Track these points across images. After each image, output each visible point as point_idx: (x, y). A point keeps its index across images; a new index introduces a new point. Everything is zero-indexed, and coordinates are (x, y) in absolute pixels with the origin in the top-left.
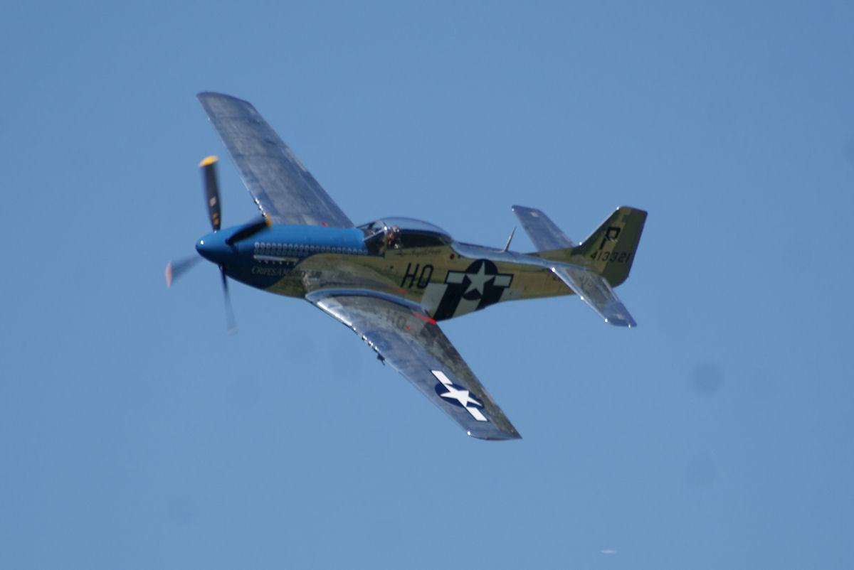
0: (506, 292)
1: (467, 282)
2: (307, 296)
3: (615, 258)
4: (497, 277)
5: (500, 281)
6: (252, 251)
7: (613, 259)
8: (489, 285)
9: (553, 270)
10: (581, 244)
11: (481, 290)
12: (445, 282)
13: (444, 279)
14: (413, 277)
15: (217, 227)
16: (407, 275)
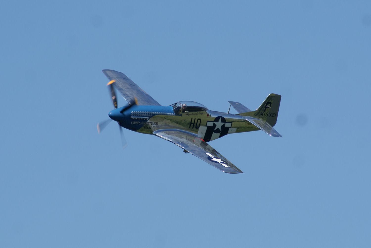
0: (230, 128)
1: (215, 126)
2: (153, 133)
3: (271, 115)
4: (226, 123)
5: (227, 125)
6: (130, 115)
7: (270, 115)
8: (223, 126)
9: (247, 120)
10: (257, 109)
11: (220, 129)
12: (206, 126)
13: (206, 125)
14: (194, 123)
15: (116, 107)
16: (191, 123)
